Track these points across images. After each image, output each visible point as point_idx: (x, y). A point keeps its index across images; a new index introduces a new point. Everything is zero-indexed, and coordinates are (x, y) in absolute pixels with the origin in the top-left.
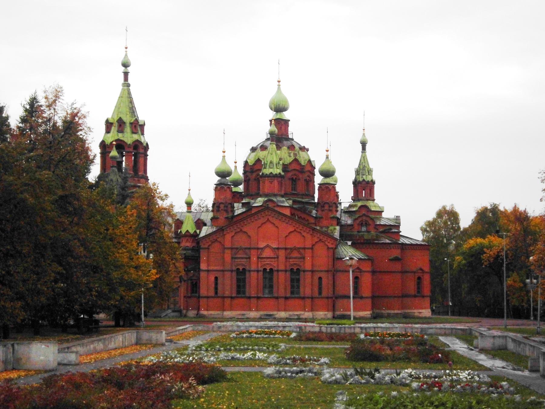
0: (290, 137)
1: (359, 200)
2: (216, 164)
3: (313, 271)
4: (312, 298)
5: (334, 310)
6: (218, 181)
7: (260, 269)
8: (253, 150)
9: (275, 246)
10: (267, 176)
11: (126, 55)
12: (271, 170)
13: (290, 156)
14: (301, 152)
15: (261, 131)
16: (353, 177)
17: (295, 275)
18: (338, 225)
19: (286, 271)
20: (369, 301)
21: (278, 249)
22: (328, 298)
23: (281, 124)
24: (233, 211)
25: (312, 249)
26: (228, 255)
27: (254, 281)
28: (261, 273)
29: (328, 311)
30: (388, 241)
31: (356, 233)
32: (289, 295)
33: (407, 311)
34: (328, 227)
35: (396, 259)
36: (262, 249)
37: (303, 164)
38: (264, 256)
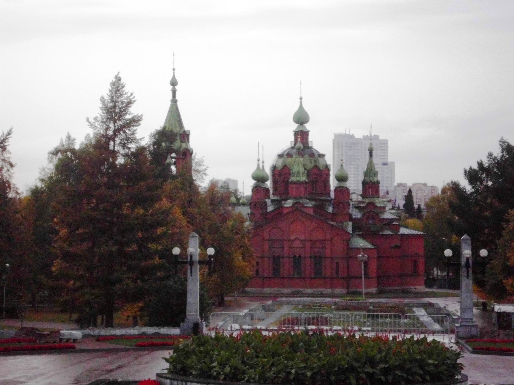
0: (310, 145)
1: (367, 198)
2: (253, 169)
3: (331, 258)
4: (331, 278)
5: (348, 288)
6: (255, 184)
7: (291, 256)
8: (280, 156)
9: (302, 238)
10: (295, 183)
11: (174, 76)
12: (298, 179)
13: (311, 163)
14: (319, 159)
15: (286, 140)
16: (361, 178)
17: (318, 259)
18: (350, 221)
19: (311, 257)
20: (375, 280)
21: (305, 240)
22: (343, 278)
23: (302, 135)
24: (266, 209)
25: (331, 240)
26: (266, 245)
27: (286, 266)
28: (292, 260)
29: (343, 288)
30: (390, 233)
31: (364, 225)
32: (313, 276)
33: (405, 287)
34: (342, 223)
35: (396, 247)
36: (292, 240)
37: (321, 168)
38: (295, 246)
